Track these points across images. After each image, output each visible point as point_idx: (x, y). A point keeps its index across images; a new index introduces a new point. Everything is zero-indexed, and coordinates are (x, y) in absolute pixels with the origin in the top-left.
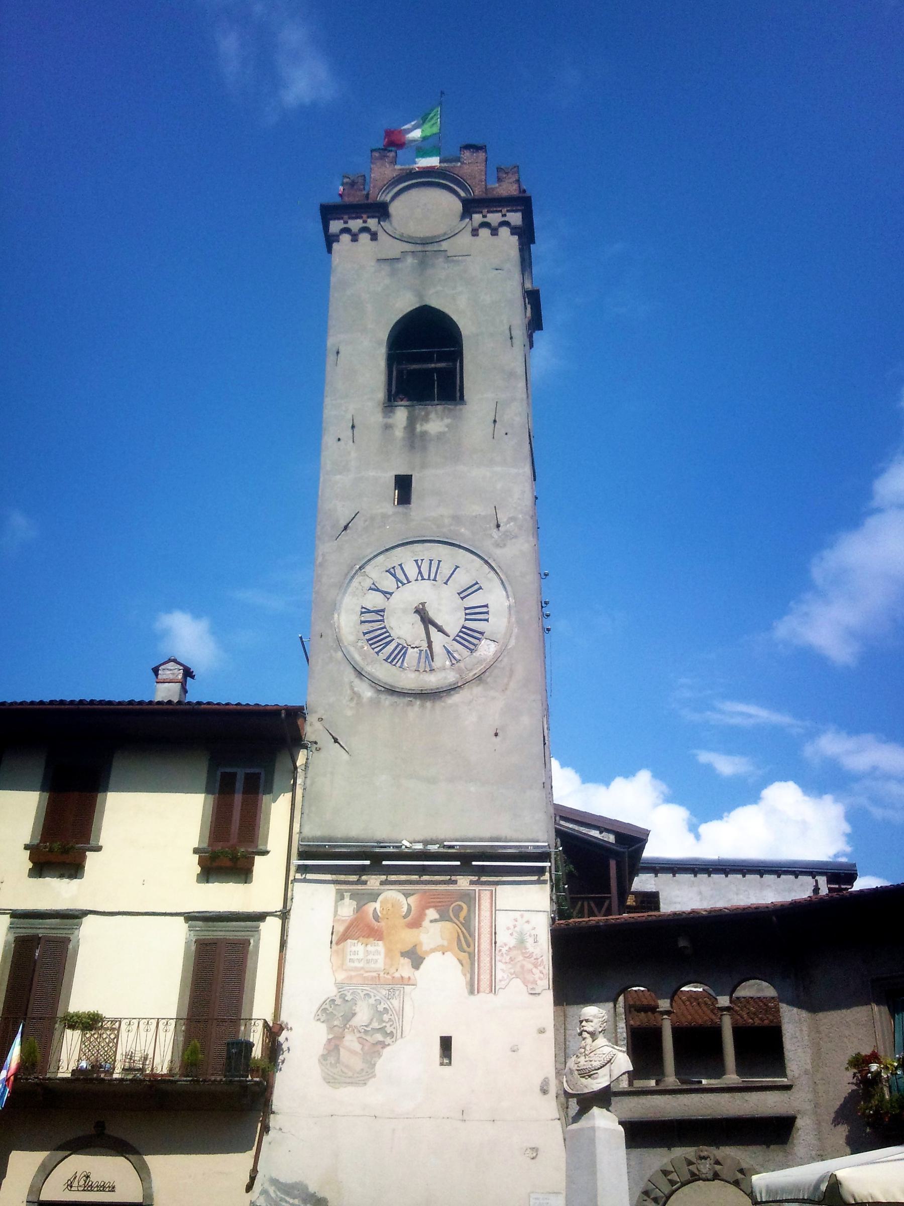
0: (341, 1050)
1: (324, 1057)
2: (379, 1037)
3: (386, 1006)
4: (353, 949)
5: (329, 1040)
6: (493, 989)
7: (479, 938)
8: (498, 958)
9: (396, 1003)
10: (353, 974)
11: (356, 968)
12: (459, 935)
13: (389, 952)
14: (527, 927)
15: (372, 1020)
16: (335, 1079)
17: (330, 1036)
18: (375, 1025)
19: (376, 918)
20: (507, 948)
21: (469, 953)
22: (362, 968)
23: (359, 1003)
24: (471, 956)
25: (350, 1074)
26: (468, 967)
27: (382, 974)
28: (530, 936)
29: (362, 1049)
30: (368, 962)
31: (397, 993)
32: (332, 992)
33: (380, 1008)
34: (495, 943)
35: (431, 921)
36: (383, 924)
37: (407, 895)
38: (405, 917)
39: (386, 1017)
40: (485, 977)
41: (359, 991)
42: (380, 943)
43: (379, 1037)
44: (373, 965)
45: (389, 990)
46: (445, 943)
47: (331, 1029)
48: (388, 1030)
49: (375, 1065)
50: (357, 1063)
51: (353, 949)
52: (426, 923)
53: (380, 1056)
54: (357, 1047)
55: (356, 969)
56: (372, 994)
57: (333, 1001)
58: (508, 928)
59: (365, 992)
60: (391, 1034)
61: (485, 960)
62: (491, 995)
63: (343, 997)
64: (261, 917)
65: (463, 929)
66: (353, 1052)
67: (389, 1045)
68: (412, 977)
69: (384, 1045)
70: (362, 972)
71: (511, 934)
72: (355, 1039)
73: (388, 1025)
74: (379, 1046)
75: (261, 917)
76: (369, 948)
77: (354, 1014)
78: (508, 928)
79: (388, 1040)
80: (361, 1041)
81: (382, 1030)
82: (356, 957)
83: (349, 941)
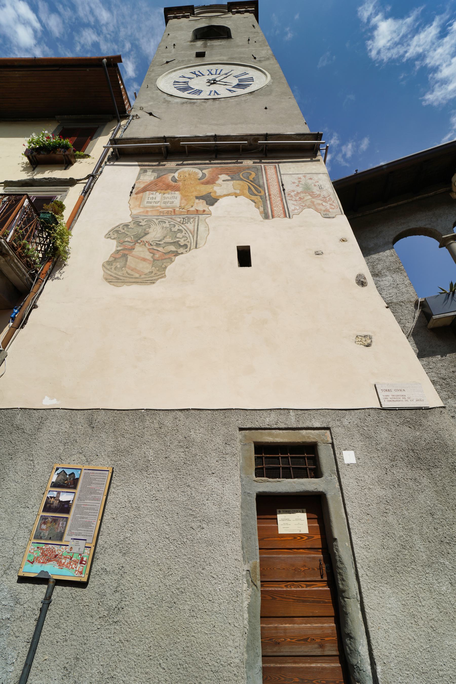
0: (129, 258)
1: (109, 263)
2: (173, 248)
3: (181, 228)
4: (151, 196)
5: (118, 251)
6: (287, 214)
7: (268, 188)
8: (287, 198)
9: (190, 226)
10: (148, 209)
11: (153, 206)
12: (249, 186)
13: (184, 197)
14: (310, 182)
15: (164, 237)
16: (118, 279)
17: (119, 248)
18: (168, 240)
19: (176, 181)
20: (295, 193)
21: (261, 196)
22: (160, 206)
23: (153, 226)
24: (264, 199)
25: (137, 275)
26: (261, 204)
27: (177, 209)
28: (315, 185)
29: (152, 257)
30: (165, 203)
31: (192, 220)
32: (128, 219)
33: (175, 229)
34: (284, 190)
35: (223, 181)
36: (180, 184)
37: (201, 169)
38: (199, 179)
39: (179, 235)
40: (278, 209)
41: (155, 220)
42: (176, 192)
43: (173, 248)
44: (169, 205)
45: (184, 218)
46: (238, 192)
47: (121, 243)
48: (182, 242)
49: (166, 267)
50: (146, 268)
51: (151, 196)
52: (219, 181)
53: (172, 261)
54: (148, 256)
55: (153, 207)
56: (167, 221)
57: (127, 226)
58: (294, 183)
59: (160, 220)
60: (185, 246)
61: (276, 200)
62: (287, 220)
63: (138, 224)
64: (72, 182)
65: (254, 184)
66: (144, 260)
67: (182, 253)
68: (207, 210)
69: (177, 254)
70: (158, 208)
71: (298, 186)
72: (146, 250)
73: (182, 240)
74: (171, 256)
75: (72, 182)
76: (166, 195)
77: (146, 234)
78: (294, 183)
79: (181, 250)
80: (152, 251)
81: (176, 244)
82: (154, 200)
83: (148, 192)
